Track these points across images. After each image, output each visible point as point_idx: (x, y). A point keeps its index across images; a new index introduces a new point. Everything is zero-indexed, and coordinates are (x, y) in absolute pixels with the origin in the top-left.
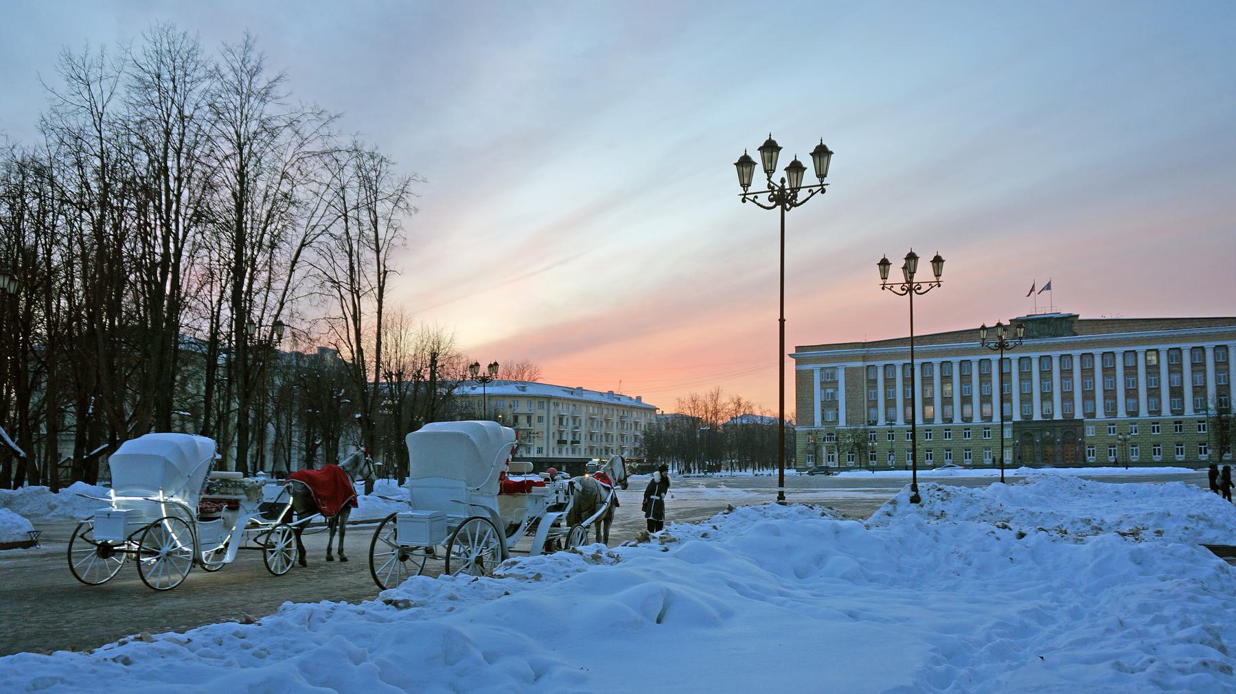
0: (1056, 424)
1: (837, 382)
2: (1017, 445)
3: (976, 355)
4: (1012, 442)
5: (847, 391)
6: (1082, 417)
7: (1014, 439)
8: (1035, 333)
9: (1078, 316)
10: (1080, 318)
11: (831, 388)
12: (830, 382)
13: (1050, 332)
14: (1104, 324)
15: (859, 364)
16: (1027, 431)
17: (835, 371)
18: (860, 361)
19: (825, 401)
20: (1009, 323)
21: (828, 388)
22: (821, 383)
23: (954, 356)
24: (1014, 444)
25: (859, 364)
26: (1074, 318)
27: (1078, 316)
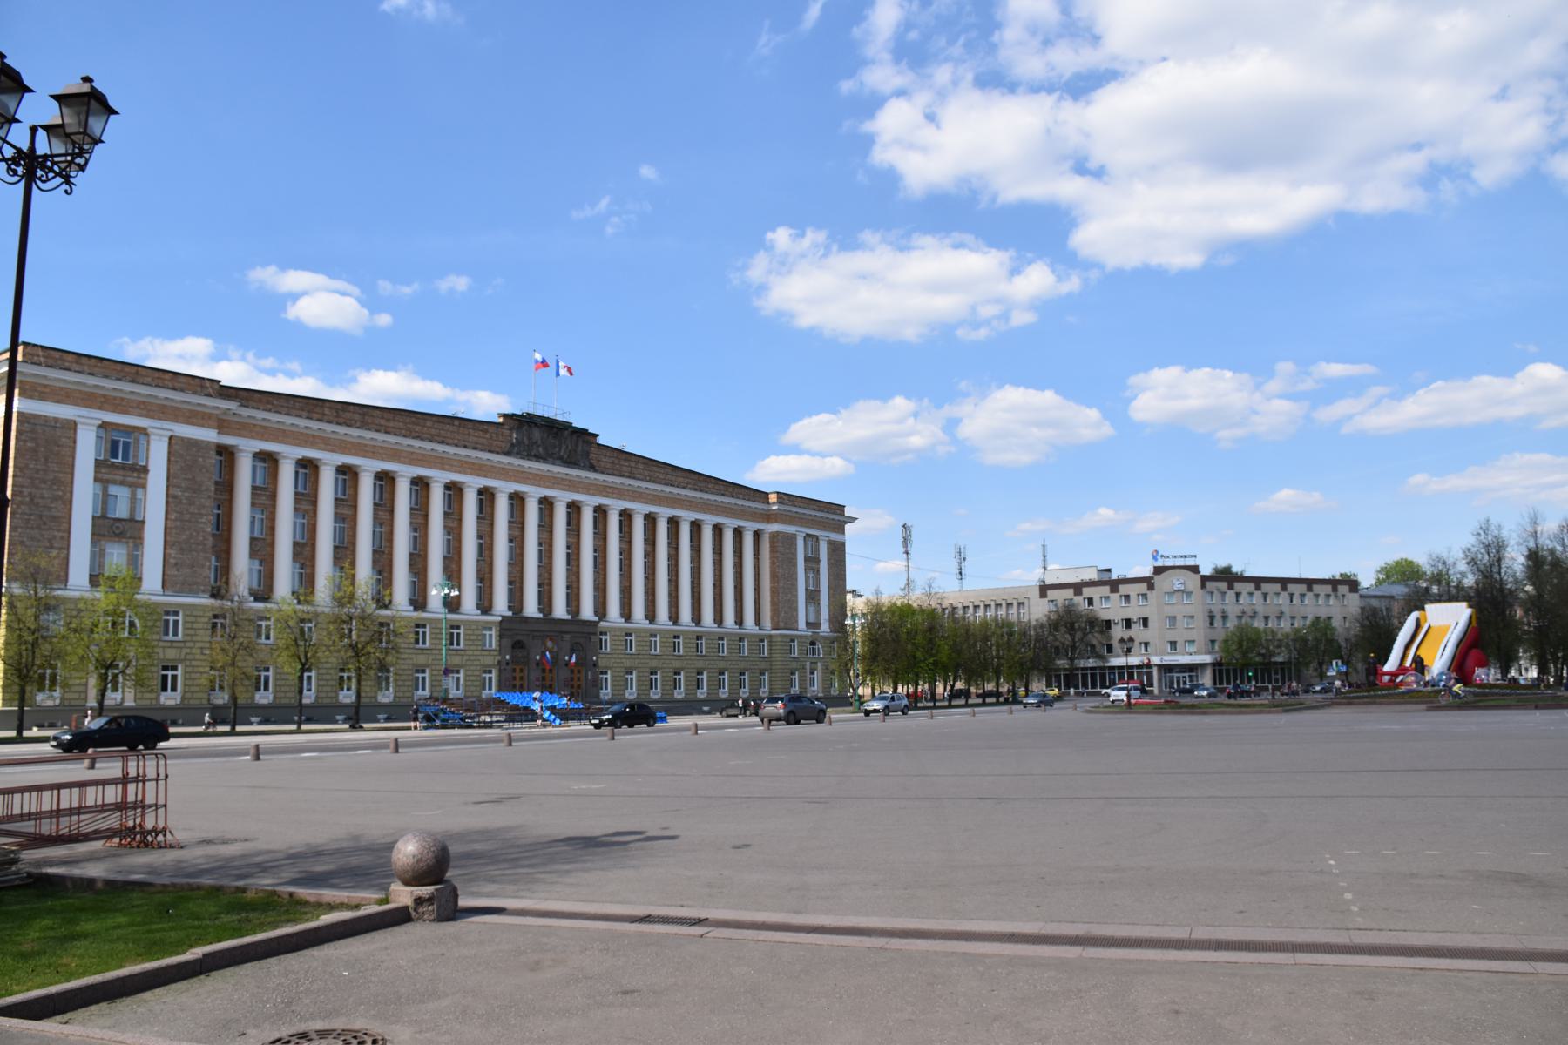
0: (565, 628)
1: (145, 470)
2: (507, 664)
3: (443, 469)
4: (498, 658)
5: (170, 497)
6: (596, 619)
7: (500, 650)
8: (541, 449)
9: (598, 435)
10: (600, 440)
11: (122, 483)
12: (123, 467)
13: (562, 454)
14: (625, 460)
15: (209, 435)
16: (519, 638)
17: (137, 441)
18: (209, 427)
19: (104, 517)
20: (501, 420)
21: (114, 482)
22: (98, 464)
23: (405, 463)
24: (499, 662)
25: (209, 435)
26: (591, 439)
27: (598, 435)
